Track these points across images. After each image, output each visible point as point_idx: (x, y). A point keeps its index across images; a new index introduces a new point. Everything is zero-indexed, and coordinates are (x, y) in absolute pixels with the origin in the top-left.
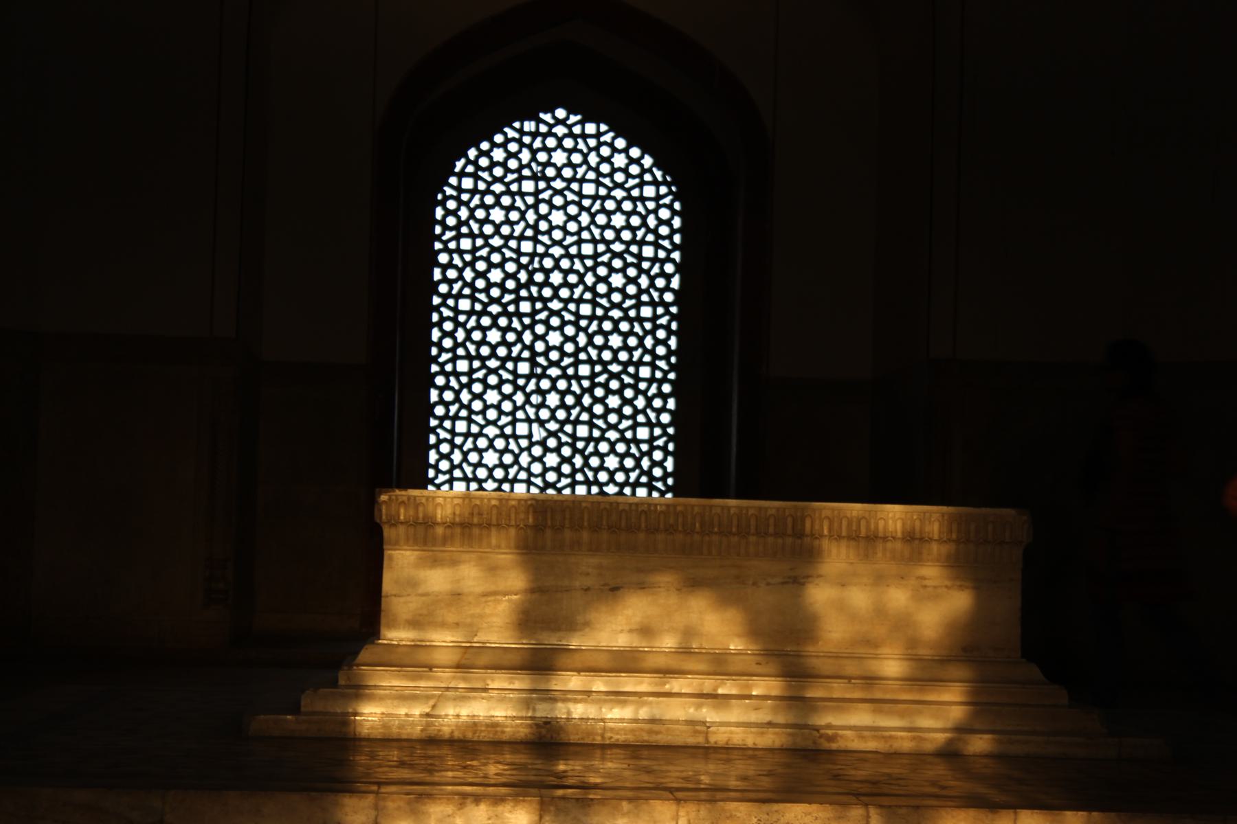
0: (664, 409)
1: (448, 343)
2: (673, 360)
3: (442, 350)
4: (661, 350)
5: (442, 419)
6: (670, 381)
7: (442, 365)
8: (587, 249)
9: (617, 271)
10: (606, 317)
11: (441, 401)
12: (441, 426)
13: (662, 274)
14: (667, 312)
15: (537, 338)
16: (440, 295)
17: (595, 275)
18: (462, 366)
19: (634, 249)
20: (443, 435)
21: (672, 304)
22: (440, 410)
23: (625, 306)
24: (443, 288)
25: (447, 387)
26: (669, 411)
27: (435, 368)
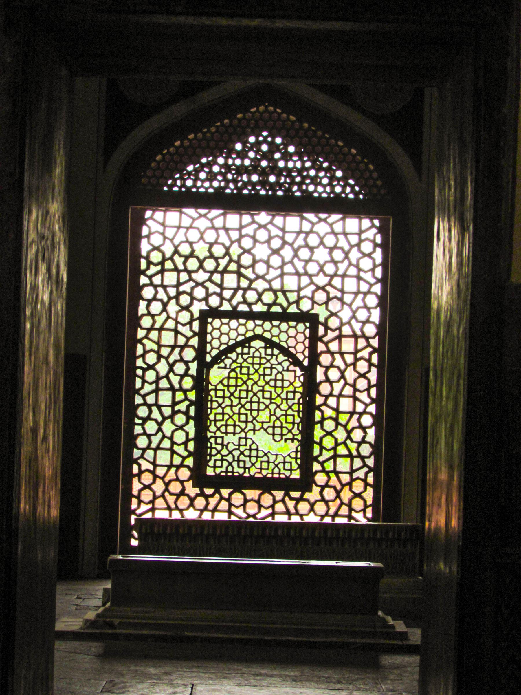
0: (368, 321)
3: (149, 263)
5: (149, 330)
7: (150, 277)
11: (149, 314)
12: (146, 337)
18: (170, 278)
20: (150, 345)
22: (146, 322)
25: (154, 299)
26: (373, 323)
27: (144, 280)
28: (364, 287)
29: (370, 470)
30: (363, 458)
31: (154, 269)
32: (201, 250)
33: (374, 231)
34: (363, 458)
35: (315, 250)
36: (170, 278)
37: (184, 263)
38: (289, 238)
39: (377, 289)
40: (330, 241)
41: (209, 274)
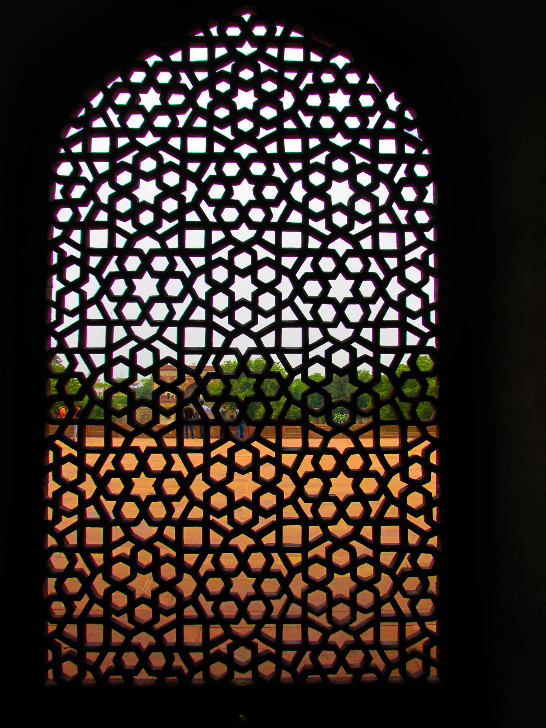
1: (72, 301)
2: (433, 317)
4: (413, 303)
6: (429, 351)
8: (293, 146)
9: (340, 177)
10: (324, 252)
13: (411, 179)
14: (421, 241)
15: (217, 288)
16: (60, 225)
17: (307, 185)
18: (96, 337)
19: (365, 143)
21: (427, 227)
23: (353, 232)
24: (64, 215)
26: (431, 399)
28: (412, 340)
29: (434, 639)
30: (421, 620)
31: (68, 321)
32: (146, 287)
33: (422, 249)
34: (421, 620)
35: (331, 282)
36: (96, 337)
37: (118, 310)
38: (288, 262)
39: (432, 342)
40: (354, 265)
41: (157, 328)
